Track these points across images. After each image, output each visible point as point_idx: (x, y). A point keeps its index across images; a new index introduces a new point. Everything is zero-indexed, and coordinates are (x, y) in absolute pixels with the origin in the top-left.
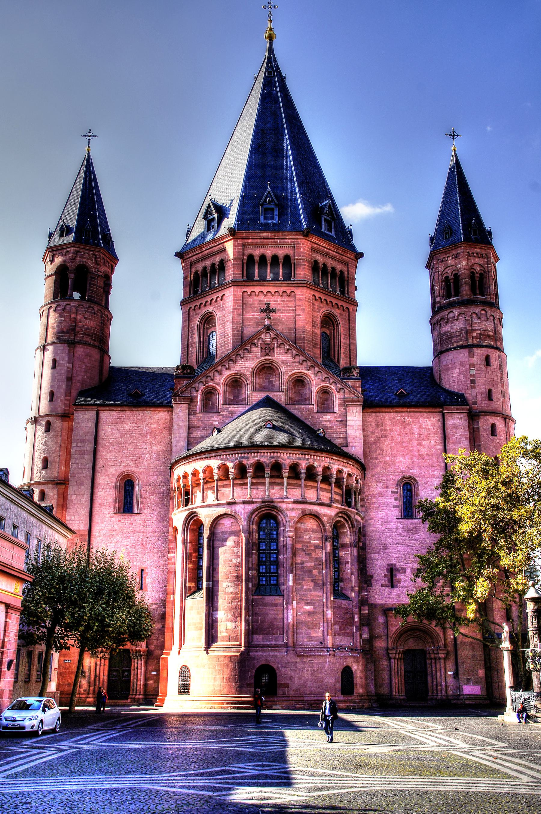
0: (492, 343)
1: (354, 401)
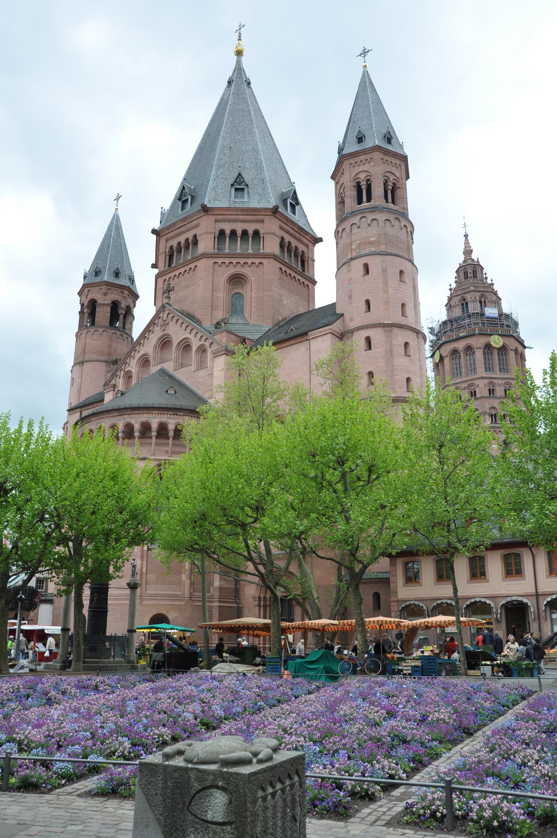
0: (373, 249)
1: (219, 352)
